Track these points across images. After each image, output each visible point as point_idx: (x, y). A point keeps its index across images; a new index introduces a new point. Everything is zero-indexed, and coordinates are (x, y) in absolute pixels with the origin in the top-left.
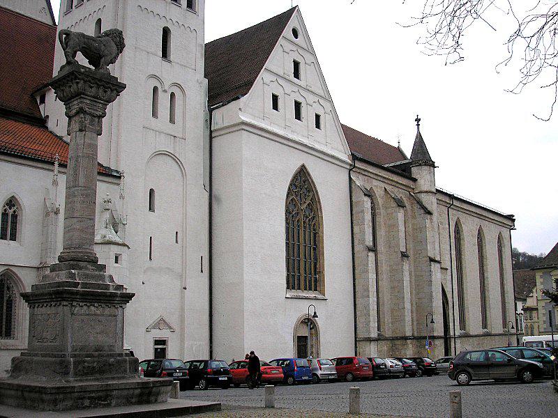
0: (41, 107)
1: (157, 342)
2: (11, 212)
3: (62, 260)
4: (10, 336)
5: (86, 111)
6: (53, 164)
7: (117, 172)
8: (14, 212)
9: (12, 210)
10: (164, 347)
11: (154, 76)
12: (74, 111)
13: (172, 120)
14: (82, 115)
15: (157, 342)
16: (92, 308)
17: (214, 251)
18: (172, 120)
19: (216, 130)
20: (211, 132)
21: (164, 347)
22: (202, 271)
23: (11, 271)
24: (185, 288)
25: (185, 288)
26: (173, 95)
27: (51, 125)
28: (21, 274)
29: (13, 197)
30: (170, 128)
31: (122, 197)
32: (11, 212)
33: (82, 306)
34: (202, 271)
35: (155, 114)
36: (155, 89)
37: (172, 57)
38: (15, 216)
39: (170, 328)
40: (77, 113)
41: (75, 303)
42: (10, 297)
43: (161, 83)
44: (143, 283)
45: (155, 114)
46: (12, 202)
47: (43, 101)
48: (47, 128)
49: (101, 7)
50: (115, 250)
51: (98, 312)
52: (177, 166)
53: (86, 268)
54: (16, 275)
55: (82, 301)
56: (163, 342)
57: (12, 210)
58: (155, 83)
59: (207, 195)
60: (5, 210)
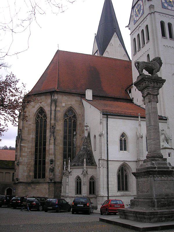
0: (130, 95)
2: (123, 139)
3: (148, 157)
4: (127, 190)
5: (150, 94)
6: (138, 117)
7: (165, 117)
8: (125, 139)
9: (124, 138)
12: (146, 94)
14: (149, 96)
16: (163, 177)
23: (126, 163)
27: (135, 101)
29: (123, 133)
31: (168, 128)
32: (123, 139)
33: (158, 177)
38: (125, 141)
40: (147, 95)
41: (155, 176)
42: (126, 174)
46: (123, 135)
47: (130, 92)
48: (133, 103)
49: (148, 49)
50: (168, 151)
51: (165, 179)
53: (159, 160)
54: (128, 165)
55: (158, 175)
57: (124, 138)
60: (121, 139)
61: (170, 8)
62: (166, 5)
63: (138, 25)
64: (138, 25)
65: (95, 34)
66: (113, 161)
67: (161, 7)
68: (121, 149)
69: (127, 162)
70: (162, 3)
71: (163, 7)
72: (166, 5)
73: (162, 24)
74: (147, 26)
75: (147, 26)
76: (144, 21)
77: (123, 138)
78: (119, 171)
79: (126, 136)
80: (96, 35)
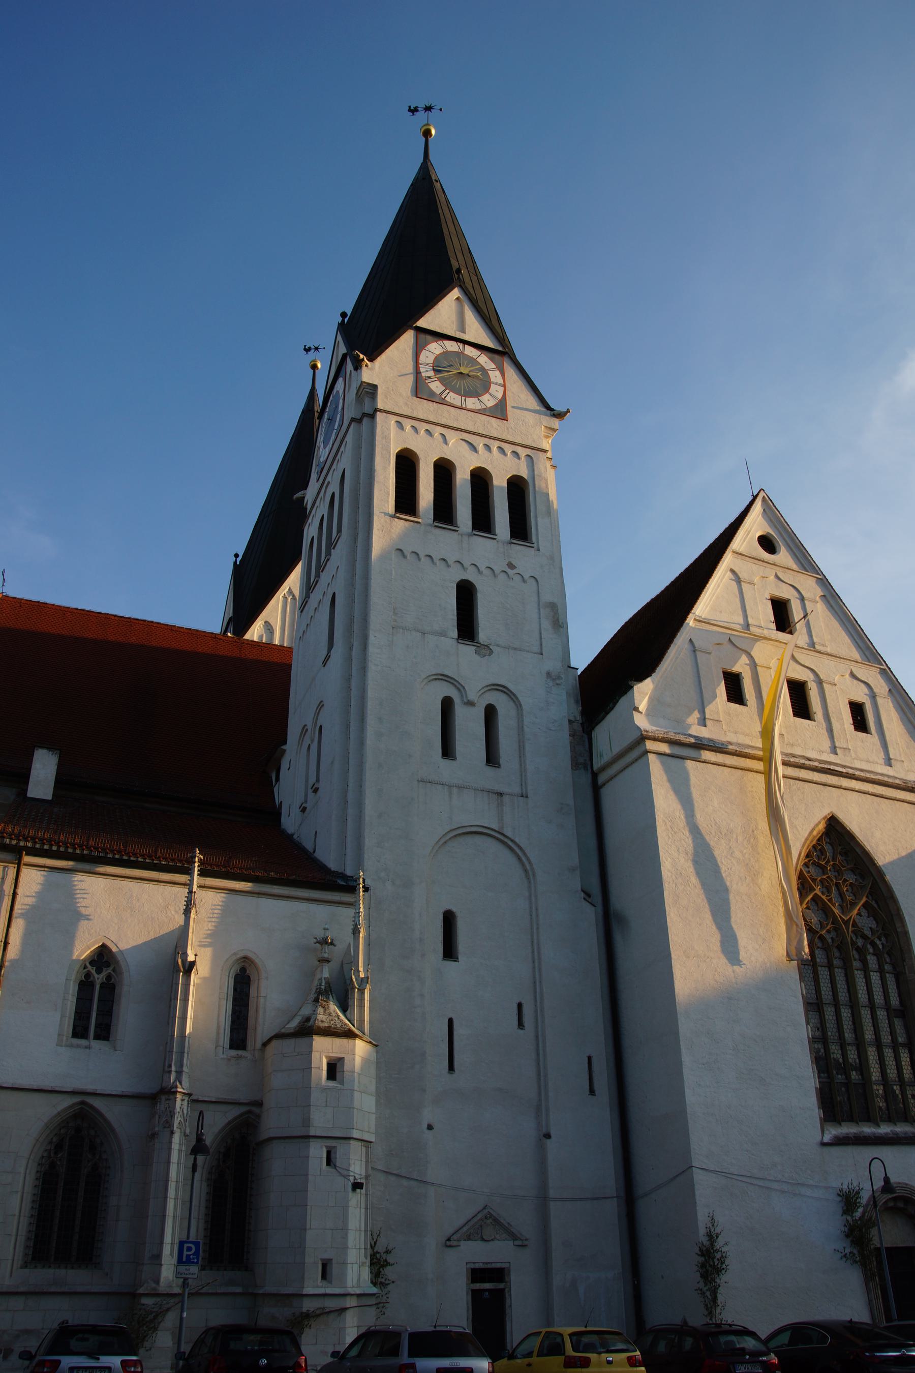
1: (477, 1274)
2: (99, 979)
8: (109, 977)
10: (501, 1286)
11: (444, 678)
13: (492, 759)
15: (477, 1274)
17: (628, 1042)
18: (492, 759)
19: (603, 769)
20: (595, 776)
21: (501, 1286)
22: (592, 1092)
23: (91, 1107)
24: (548, 1136)
25: (548, 1136)
26: (490, 713)
28: (113, 1113)
30: (489, 777)
34: (592, 1092)
35: (448, 751)
36: (447, 706)
37: (483, 635)
39: (514, 1236)
43: (460, 688)
44: (430, 1127)
45: (448, 751)
47: (278, 779)
52: (507, 852)
54: (101, 1115)
56: (497, 1274)
58: (448, 690)
59: (590, 915)
60: (88, 975)
61: (453, 398)
62: (436, 387)
65: (236, 556)
66: (15, 1093)
68: (79, 1031)
69: (97, 1103)
72: (436, 387)
77: (99, 971)
78: (58, 1147)
79: (117, 962)
80: (239, 560)
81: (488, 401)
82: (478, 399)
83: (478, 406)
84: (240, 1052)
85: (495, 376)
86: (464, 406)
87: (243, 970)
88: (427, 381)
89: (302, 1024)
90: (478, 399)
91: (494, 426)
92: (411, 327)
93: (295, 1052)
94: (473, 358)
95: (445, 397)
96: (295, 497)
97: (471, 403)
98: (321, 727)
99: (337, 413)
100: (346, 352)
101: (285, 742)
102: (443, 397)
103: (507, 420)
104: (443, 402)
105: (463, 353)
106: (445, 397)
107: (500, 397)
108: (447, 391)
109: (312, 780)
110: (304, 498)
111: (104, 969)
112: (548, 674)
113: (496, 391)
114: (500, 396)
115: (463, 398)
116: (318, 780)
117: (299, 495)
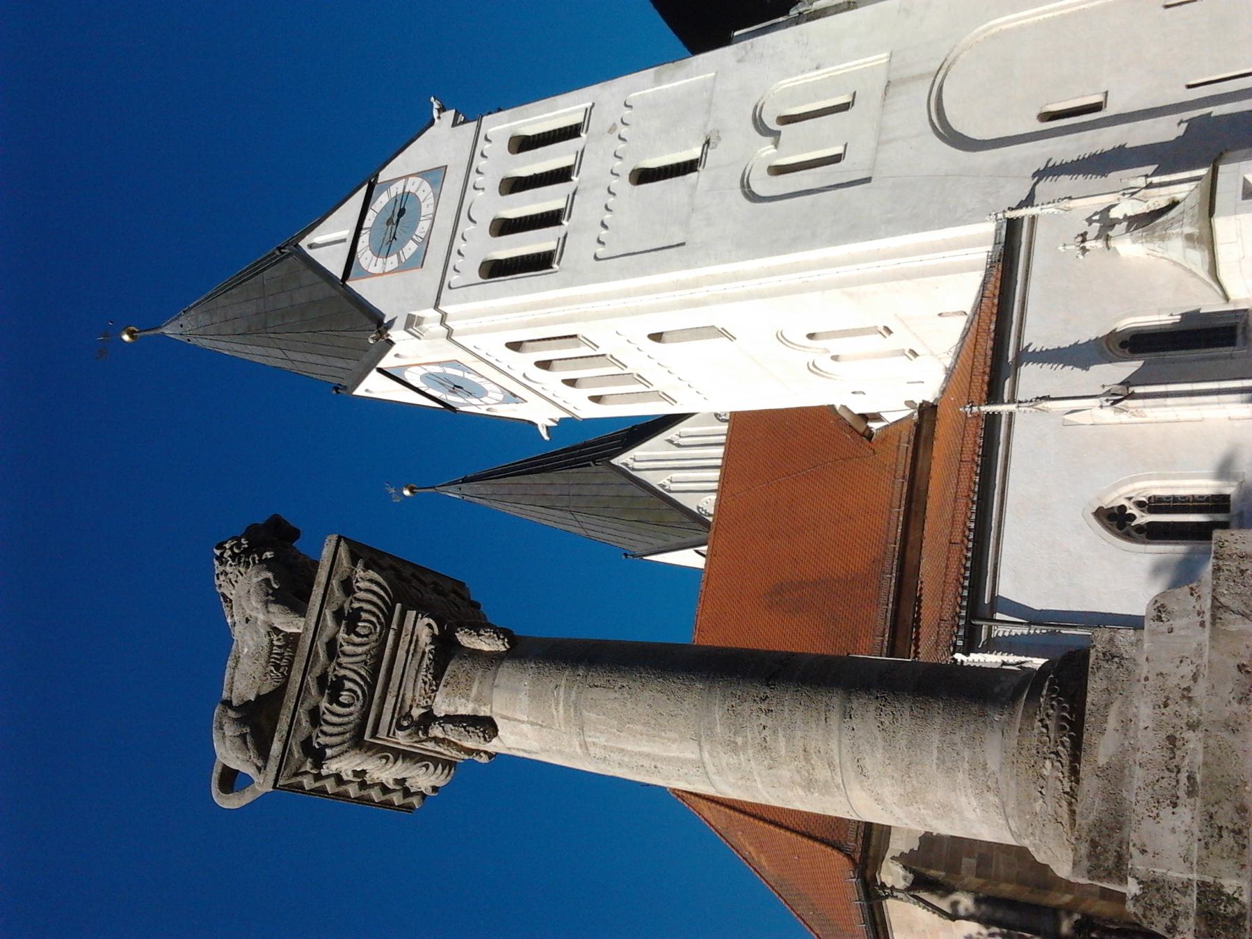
0: (891, 418)
6: (993, 419)
27: (929, 392)
47: (877, 417)
53: (1114, 775)
61: (423, 226)
62: (410, 248)
63: (518, 381)
64: (518, 381)
67: (417, 273)
70: (403, 267)
71: (418, 261)
73: (496, 269)
74: (515, 346)
75: (515, 346)
76: (492, 360)
81: (422, 190)
82: (423, 201)
83: (432, 201)
84: (1239, 331)
85: (396, 189)
86: (431, 216)
87: (1123, 345)
88: (403, 260)
89: (1196, 243)
90: (423, 201)
91: (452, 185)
92: (344, 285)
93: (1236, 242)
94: (377, 216)
95: (421, 238)
96: (547, 438)
97: (426, 210)
98: (811, 336)
99: (445, 373)
100: (375, 370)
101: (832, 407)
102: (421, 240)
103: (446, 167)
104: (427, 240)
105: (371, 228)
106: (421, 238)
107: (420, 179)
108: (414, 237)
109: (876, 343)
110: (547, 427)
111: (1129, 511)
112: (739, 61)
113: (414, 185)
114: (418, 180)
115: (422, 218)
116: (872, 330)
117: (544, 433)
